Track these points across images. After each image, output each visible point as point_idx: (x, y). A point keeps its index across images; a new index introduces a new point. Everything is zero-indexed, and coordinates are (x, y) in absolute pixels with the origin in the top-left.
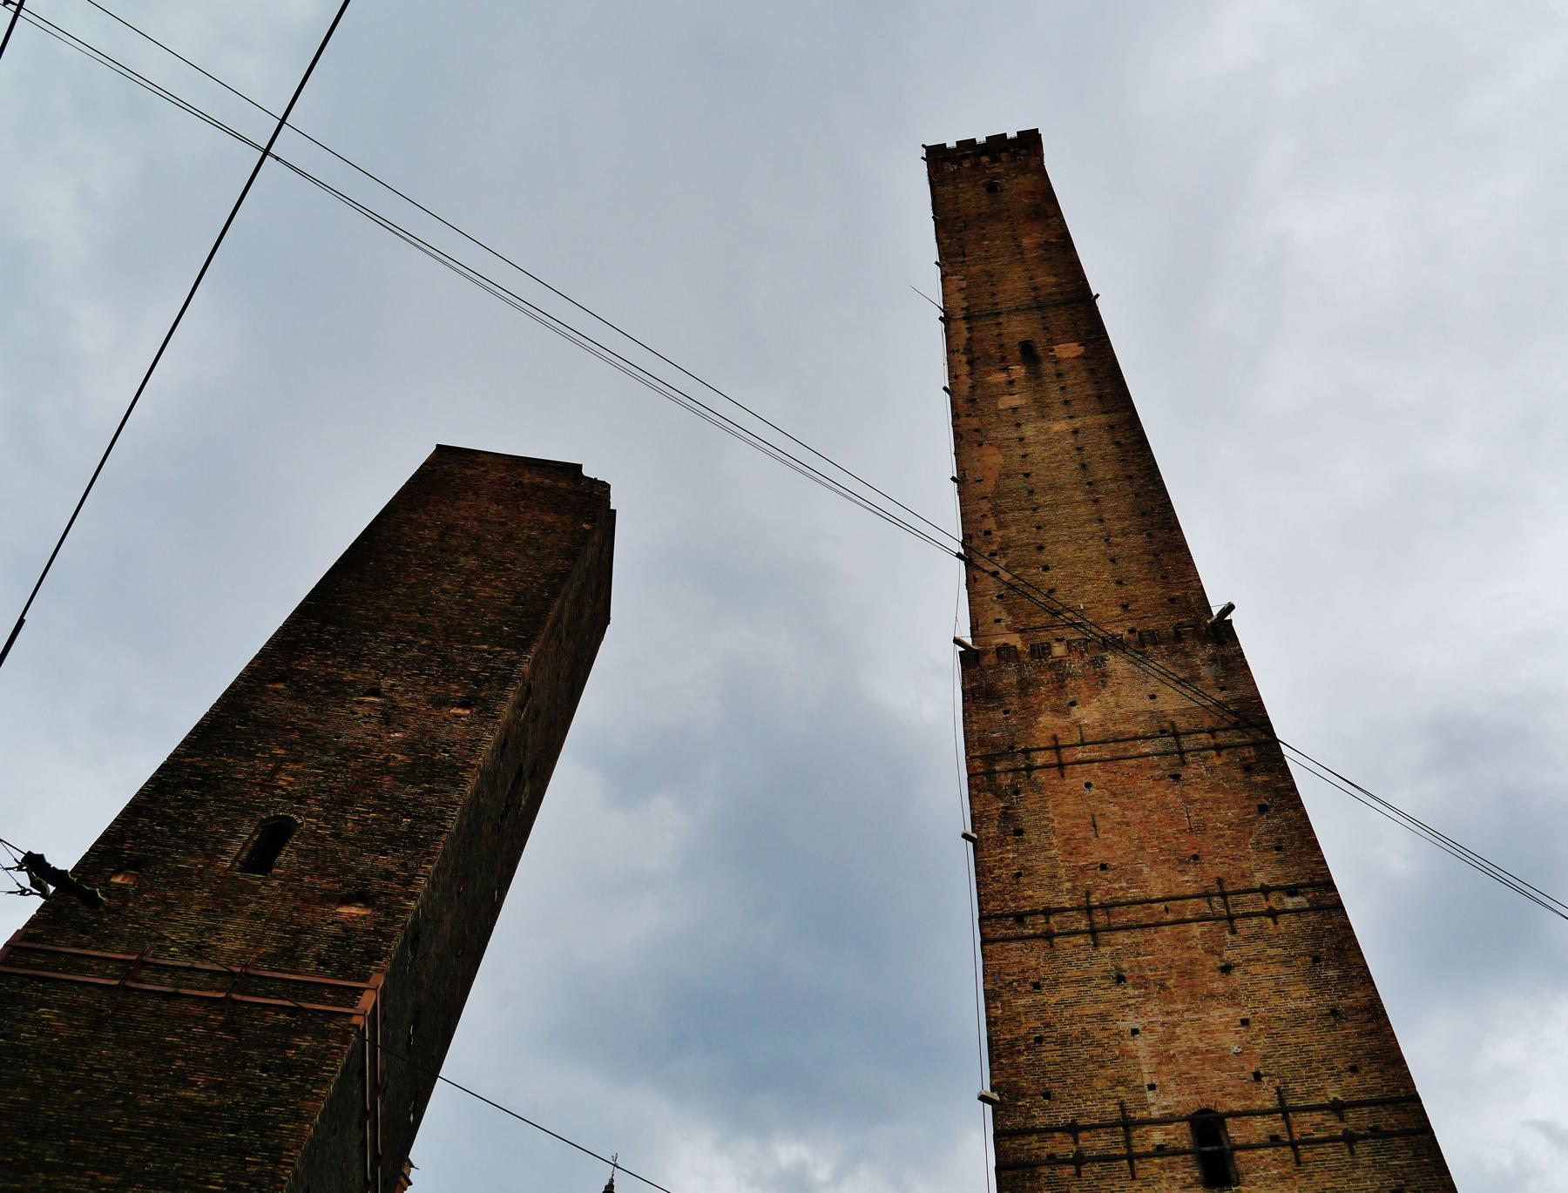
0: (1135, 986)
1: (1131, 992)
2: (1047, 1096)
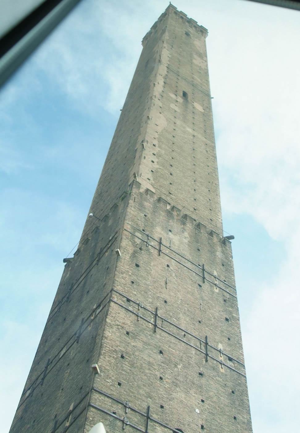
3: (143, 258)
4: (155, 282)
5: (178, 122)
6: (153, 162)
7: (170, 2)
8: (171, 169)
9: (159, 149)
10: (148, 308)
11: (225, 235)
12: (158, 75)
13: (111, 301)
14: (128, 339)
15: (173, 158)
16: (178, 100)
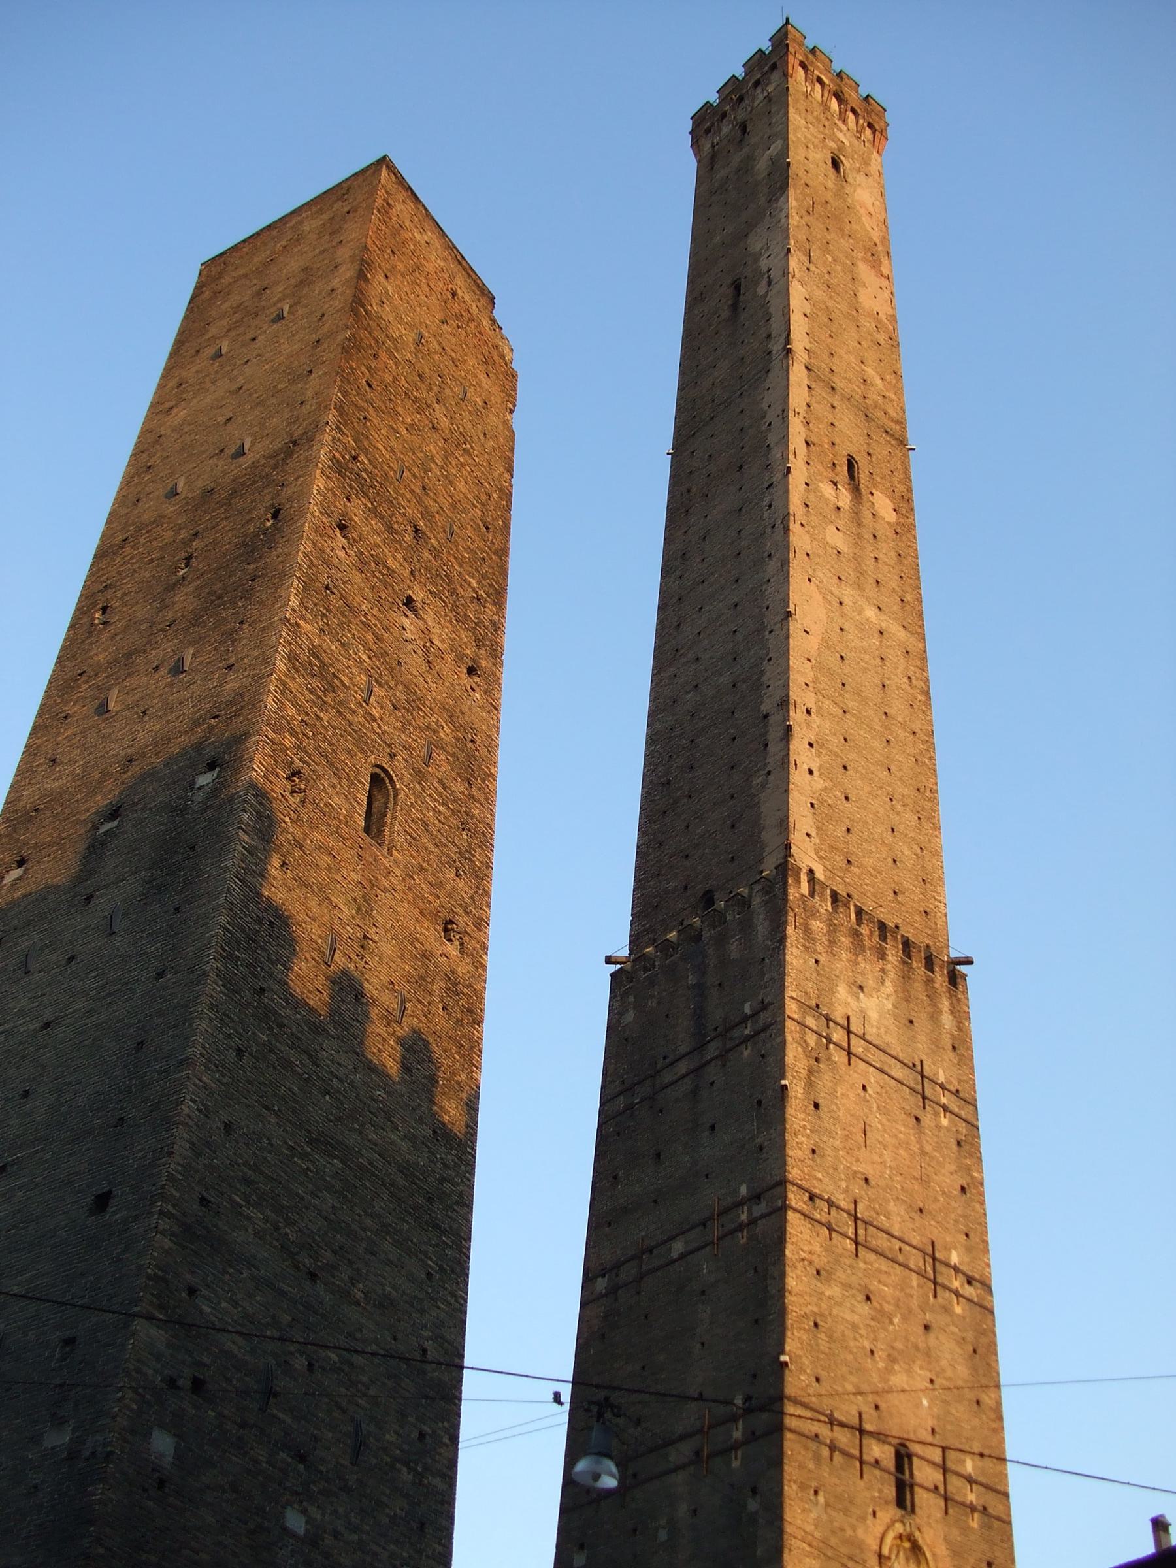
6: (811, 772)
7: (787, 19)
9: (818, 720)
10: (843, 1204)
11: (954, 954)
12: (791, 414)
14: (819, 1284)
15: (846, 740)
16: (840, 504)
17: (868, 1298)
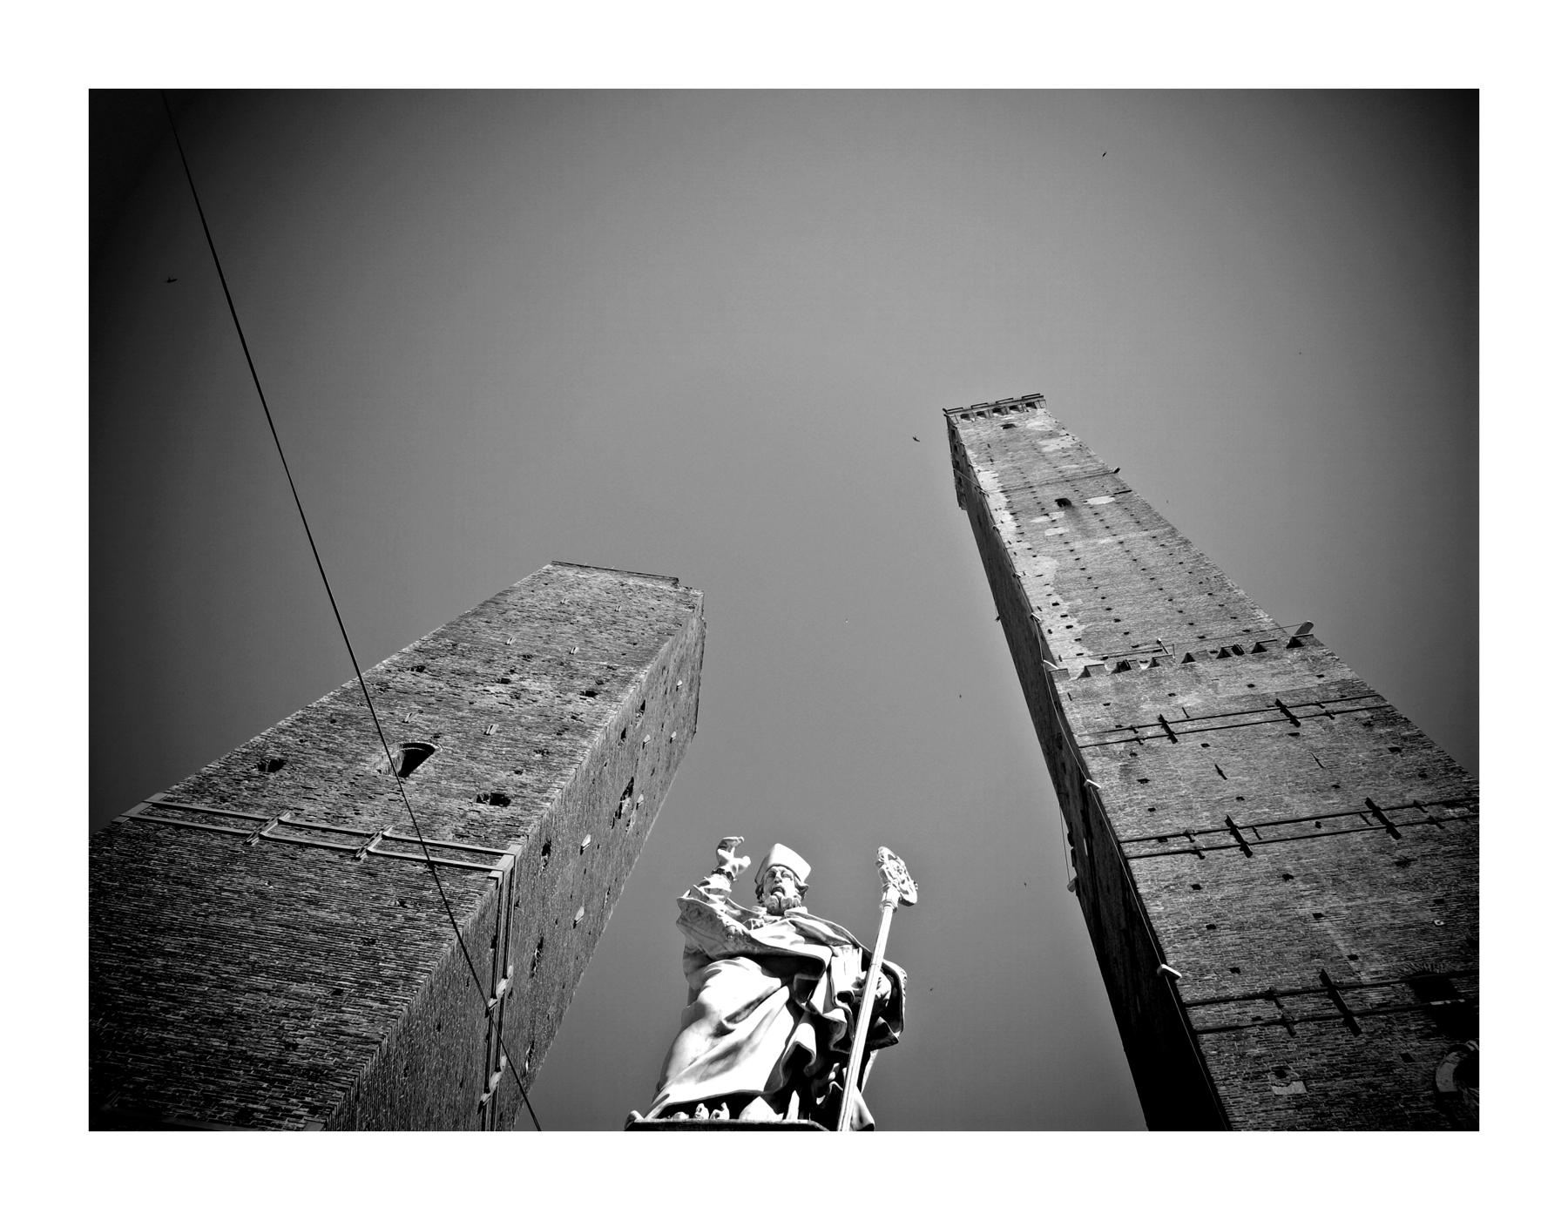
0: (1305, 882)
1: (1302, 887)
2: (1235, 970)
3: (1145, 764)
4: (1195, 784)
5: (1077, 545)
8: (1113, 614)
13: (1126, 859)
17: (1287, 877)
